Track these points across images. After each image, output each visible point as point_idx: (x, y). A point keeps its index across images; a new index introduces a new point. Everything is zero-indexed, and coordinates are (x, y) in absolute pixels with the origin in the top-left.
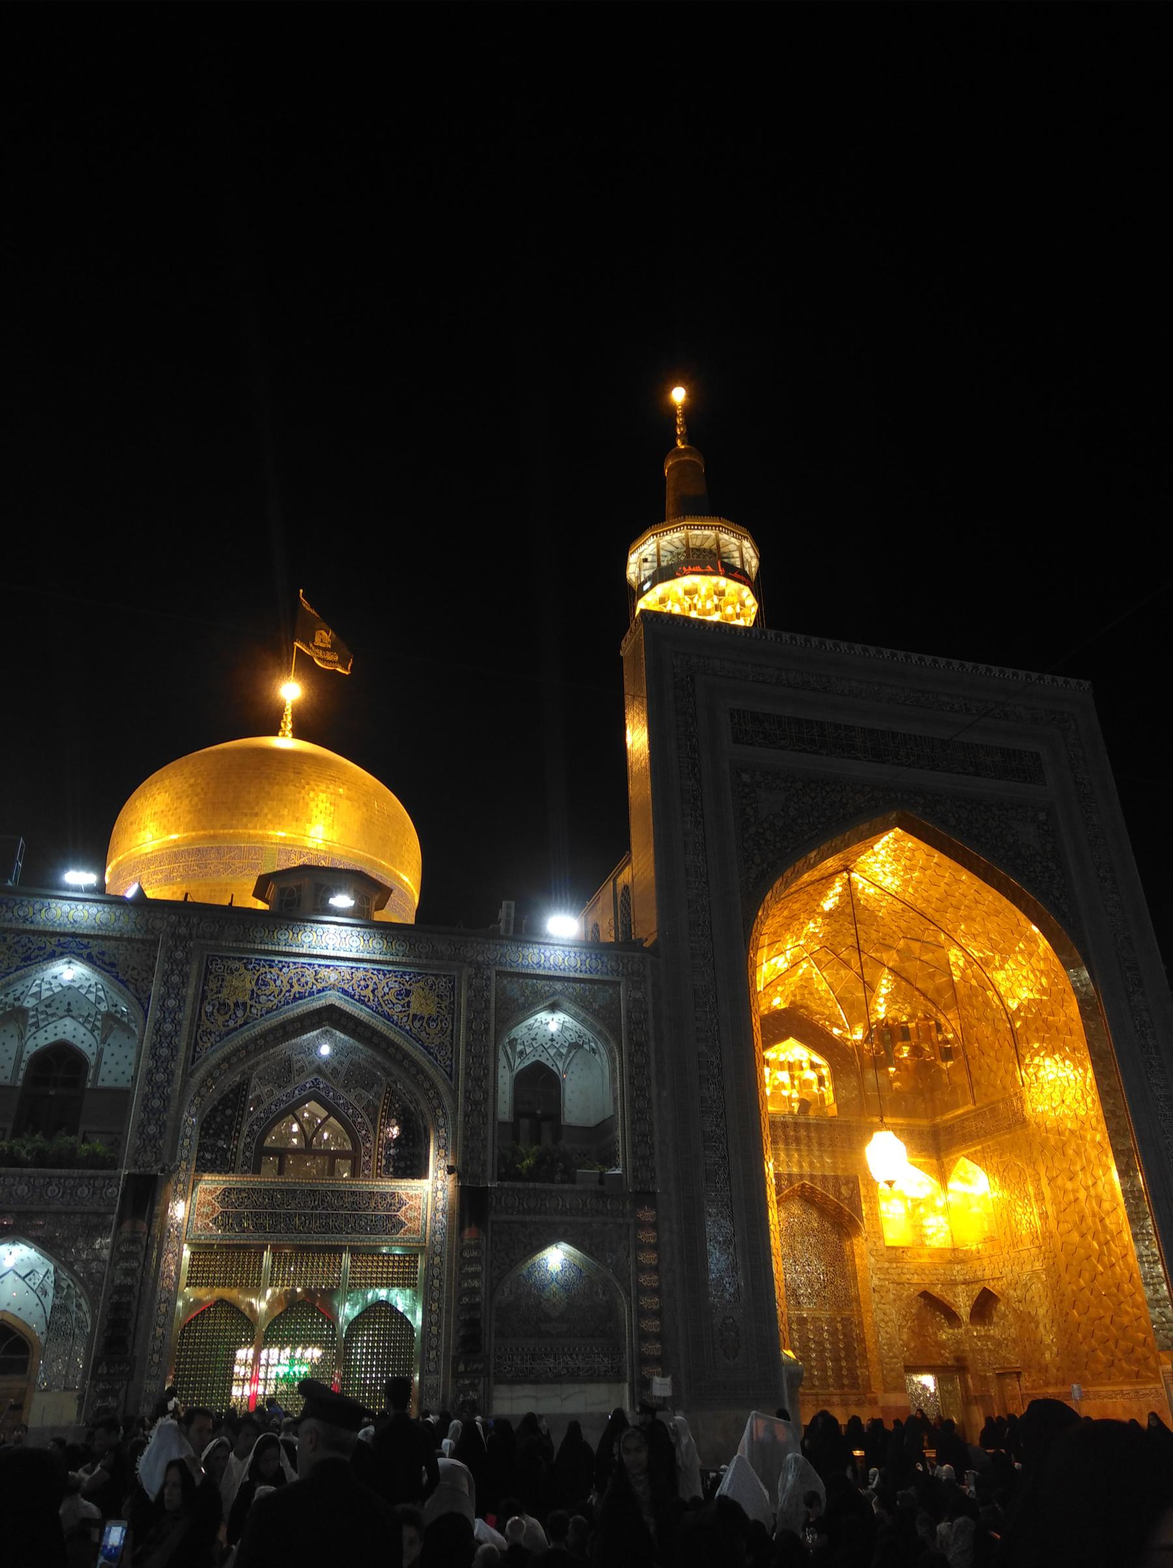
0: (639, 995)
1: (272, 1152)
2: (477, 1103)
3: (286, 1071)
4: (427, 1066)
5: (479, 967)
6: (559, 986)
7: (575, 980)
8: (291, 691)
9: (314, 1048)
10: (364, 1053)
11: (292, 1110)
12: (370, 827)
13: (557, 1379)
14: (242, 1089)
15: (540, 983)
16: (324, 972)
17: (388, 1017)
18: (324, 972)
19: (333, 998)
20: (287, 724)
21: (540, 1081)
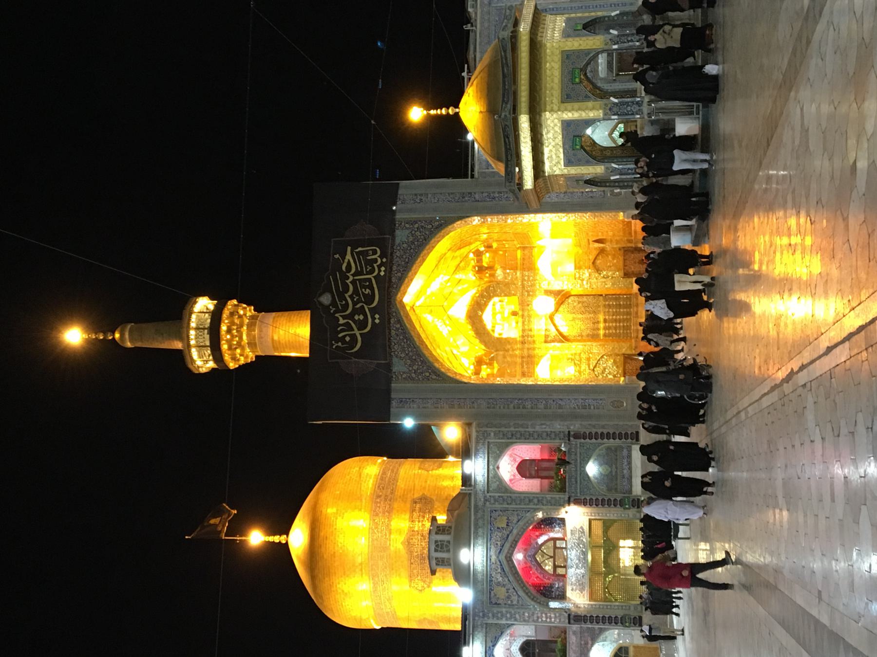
0: (492, 434)
1: (555, 570)
2: (538, 501)
3: (527, 569)
4: (526, 520)
5: (486, 500)
6: (491, 467)
7: (488, 461)
8: (256, 538)
9: (519, 561)
10: (520, 545)
11: (539, 565)
12: (351, 498)
13: (630, 469)
14: (535, 586)
15: (491, 475)
16: (493, 560)
17: (508, 535)
18: (493, 560)
19: (502, 557)
20: (276, 539)
21: (525, 469)
